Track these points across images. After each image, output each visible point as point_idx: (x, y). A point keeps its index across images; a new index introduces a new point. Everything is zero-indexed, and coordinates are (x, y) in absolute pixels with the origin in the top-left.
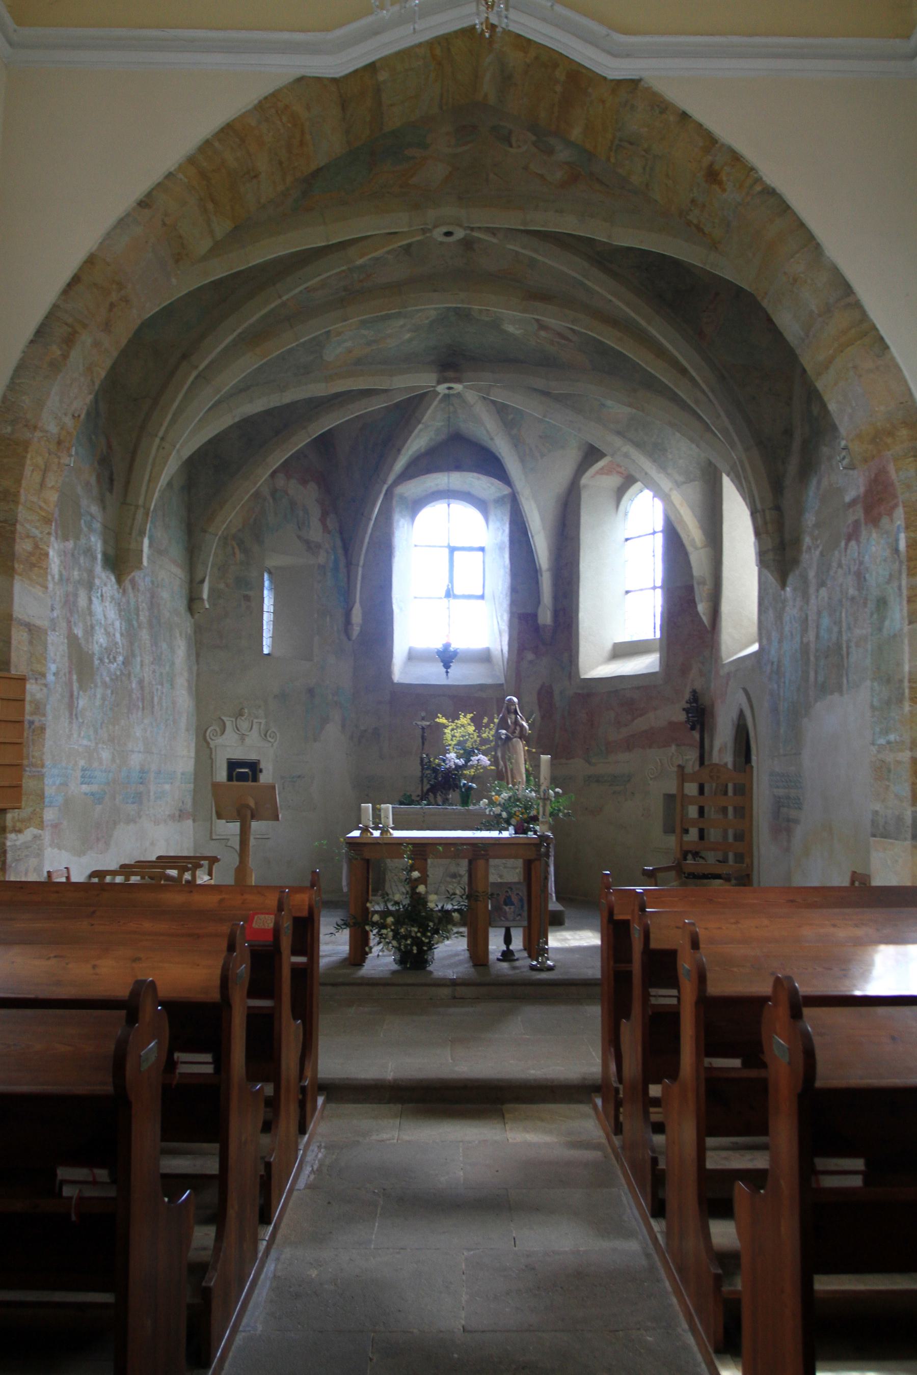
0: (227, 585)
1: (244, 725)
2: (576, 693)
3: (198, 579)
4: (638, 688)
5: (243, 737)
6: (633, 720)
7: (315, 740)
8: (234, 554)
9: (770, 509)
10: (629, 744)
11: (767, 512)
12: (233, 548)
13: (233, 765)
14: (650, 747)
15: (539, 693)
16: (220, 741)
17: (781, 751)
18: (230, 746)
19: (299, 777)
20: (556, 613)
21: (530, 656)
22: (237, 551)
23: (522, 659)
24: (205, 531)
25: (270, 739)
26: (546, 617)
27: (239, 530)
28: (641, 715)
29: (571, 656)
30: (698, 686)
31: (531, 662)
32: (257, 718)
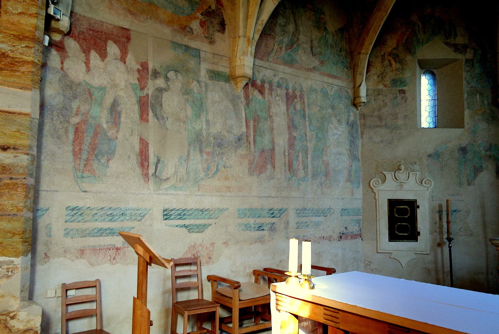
0: (385, 86)
1: (402, 176)
3: (358, 85)
5: (401, 185)
7: (469, 184)
8: (391, 65)
12: (390, 61)
13: (393, 204)
16: (382, 187)
18: (390, 189)
19: (455, 211)
22: (393, 62)
24: (359, 53)
25: (425, 185)
27: (394, 49)
32: (413, 171)
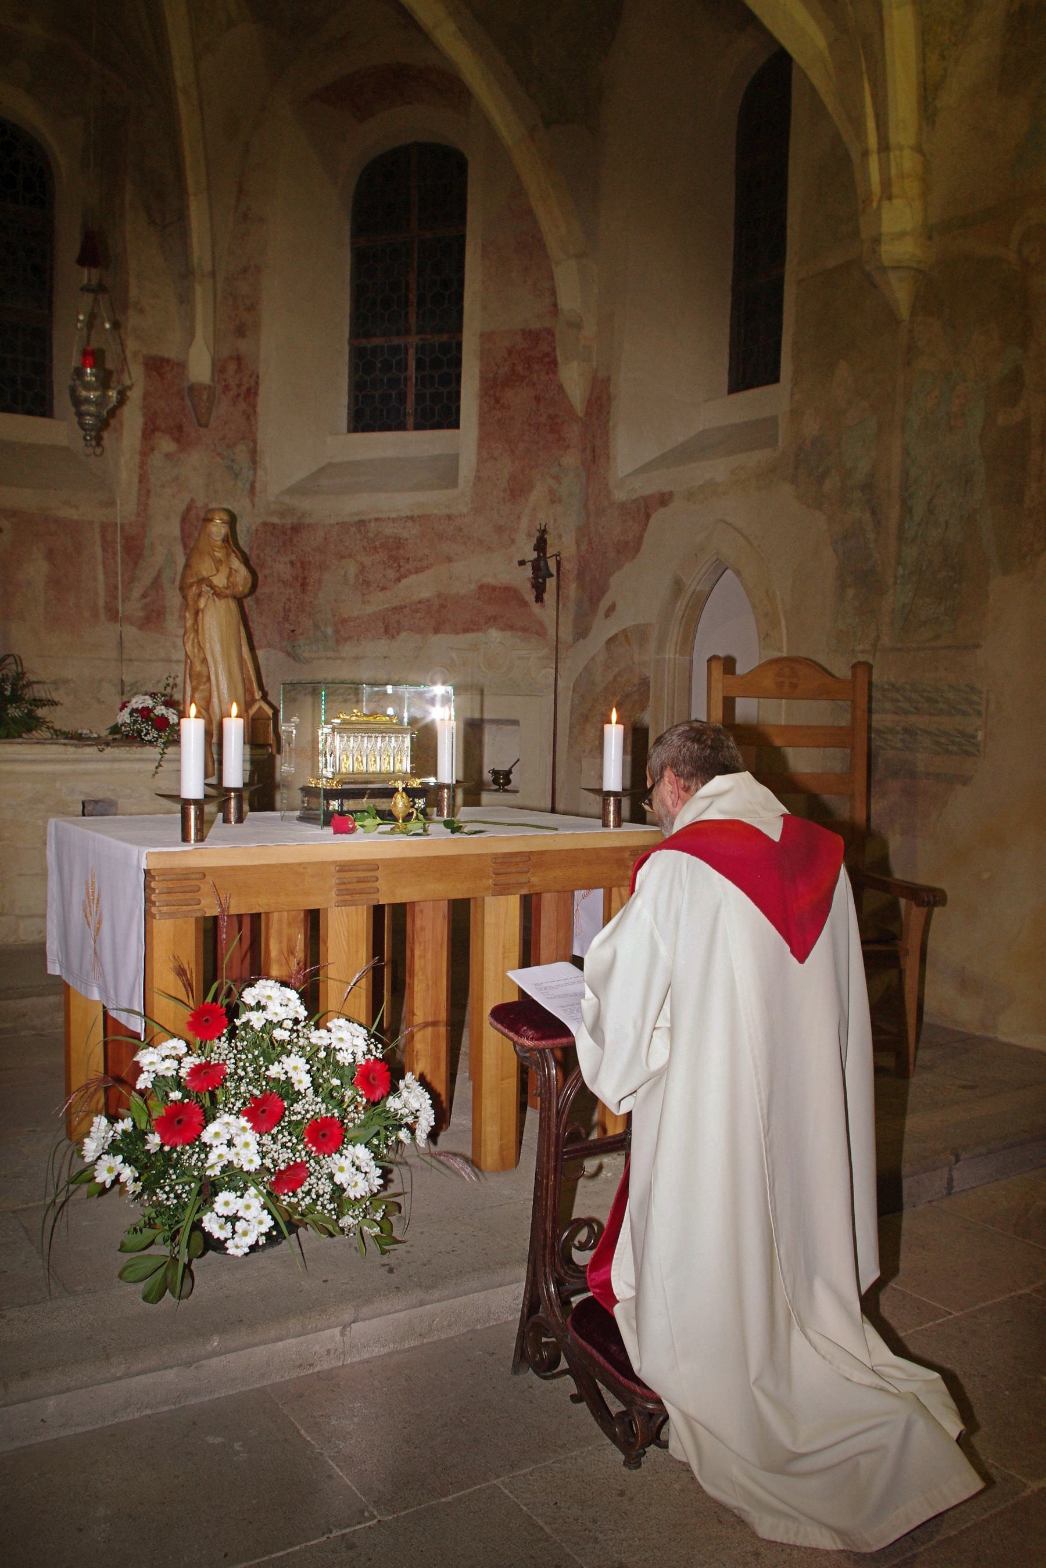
2: (265, 524)
4: (412, 518)
6: (399, 580)
9: (912, 148)
10: (389, 625)
11: (907, 152)
14: (436, 631)
15: (184, 519)
17: (886, 641)
20: (219, 368)
21: (166, 445)
23: (153, 449)
26: (200, 368)
28: (418, 571)
29: (253, 452)
30: (543, 518)
31: (168, 456)
